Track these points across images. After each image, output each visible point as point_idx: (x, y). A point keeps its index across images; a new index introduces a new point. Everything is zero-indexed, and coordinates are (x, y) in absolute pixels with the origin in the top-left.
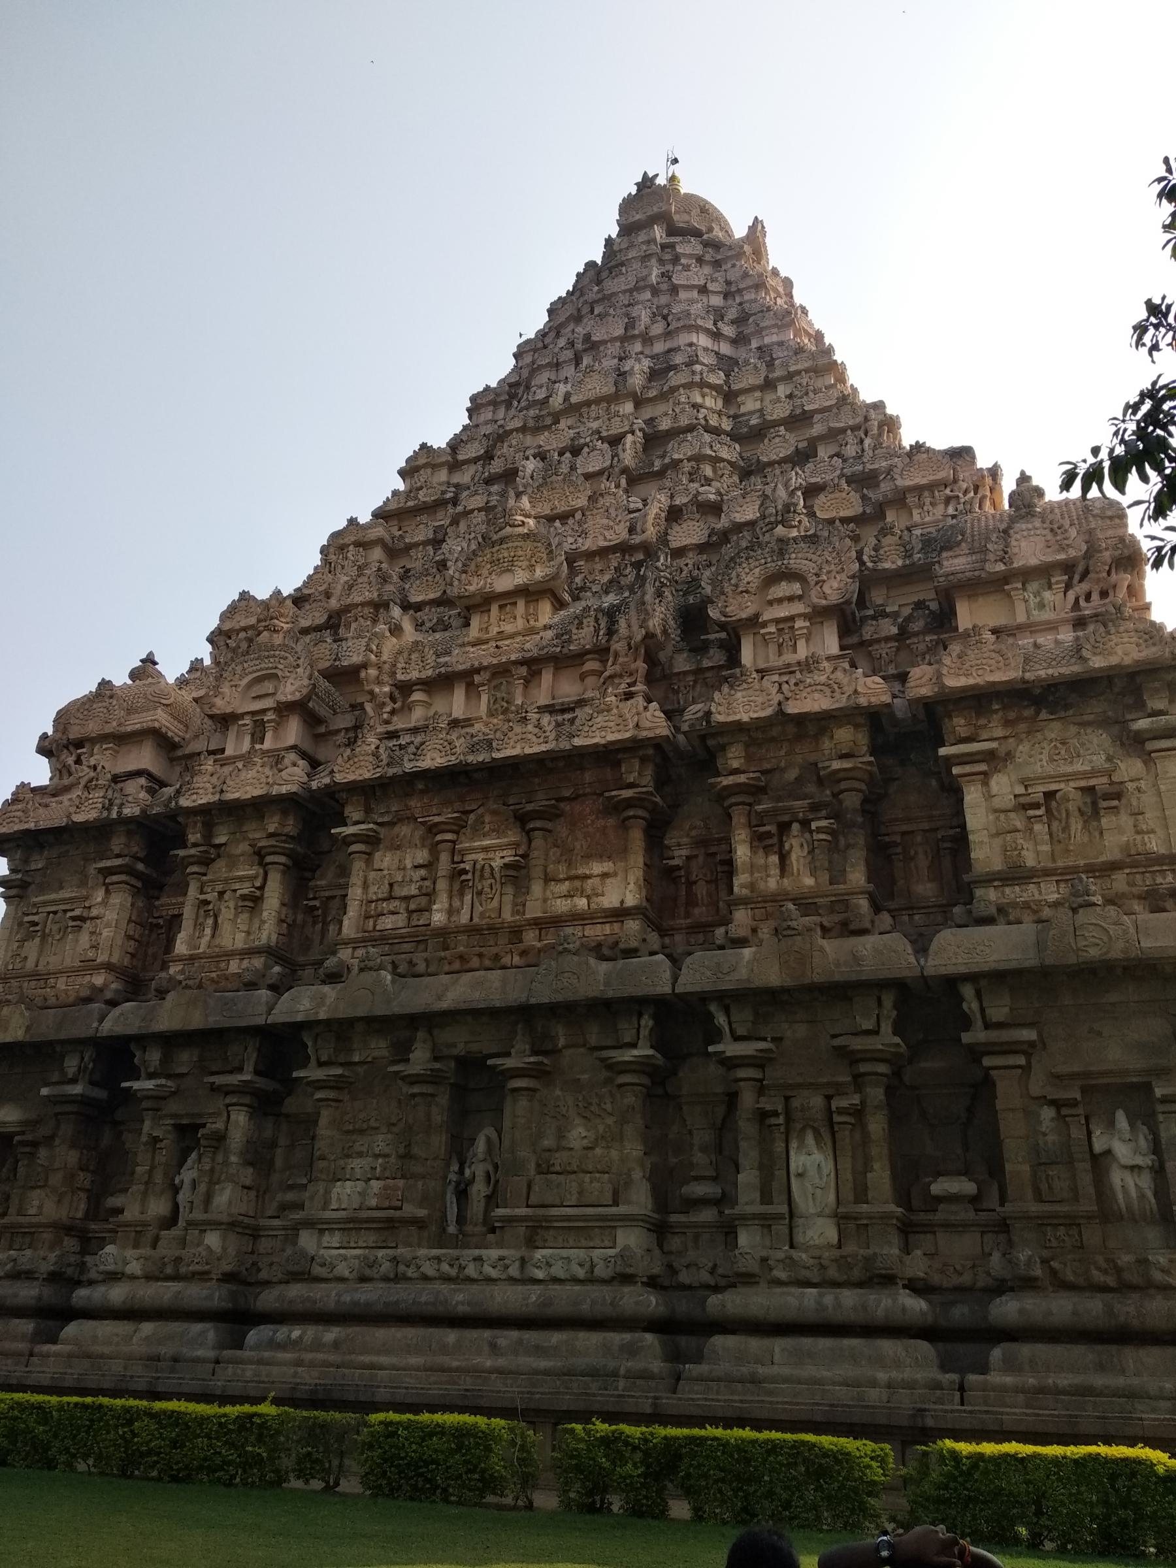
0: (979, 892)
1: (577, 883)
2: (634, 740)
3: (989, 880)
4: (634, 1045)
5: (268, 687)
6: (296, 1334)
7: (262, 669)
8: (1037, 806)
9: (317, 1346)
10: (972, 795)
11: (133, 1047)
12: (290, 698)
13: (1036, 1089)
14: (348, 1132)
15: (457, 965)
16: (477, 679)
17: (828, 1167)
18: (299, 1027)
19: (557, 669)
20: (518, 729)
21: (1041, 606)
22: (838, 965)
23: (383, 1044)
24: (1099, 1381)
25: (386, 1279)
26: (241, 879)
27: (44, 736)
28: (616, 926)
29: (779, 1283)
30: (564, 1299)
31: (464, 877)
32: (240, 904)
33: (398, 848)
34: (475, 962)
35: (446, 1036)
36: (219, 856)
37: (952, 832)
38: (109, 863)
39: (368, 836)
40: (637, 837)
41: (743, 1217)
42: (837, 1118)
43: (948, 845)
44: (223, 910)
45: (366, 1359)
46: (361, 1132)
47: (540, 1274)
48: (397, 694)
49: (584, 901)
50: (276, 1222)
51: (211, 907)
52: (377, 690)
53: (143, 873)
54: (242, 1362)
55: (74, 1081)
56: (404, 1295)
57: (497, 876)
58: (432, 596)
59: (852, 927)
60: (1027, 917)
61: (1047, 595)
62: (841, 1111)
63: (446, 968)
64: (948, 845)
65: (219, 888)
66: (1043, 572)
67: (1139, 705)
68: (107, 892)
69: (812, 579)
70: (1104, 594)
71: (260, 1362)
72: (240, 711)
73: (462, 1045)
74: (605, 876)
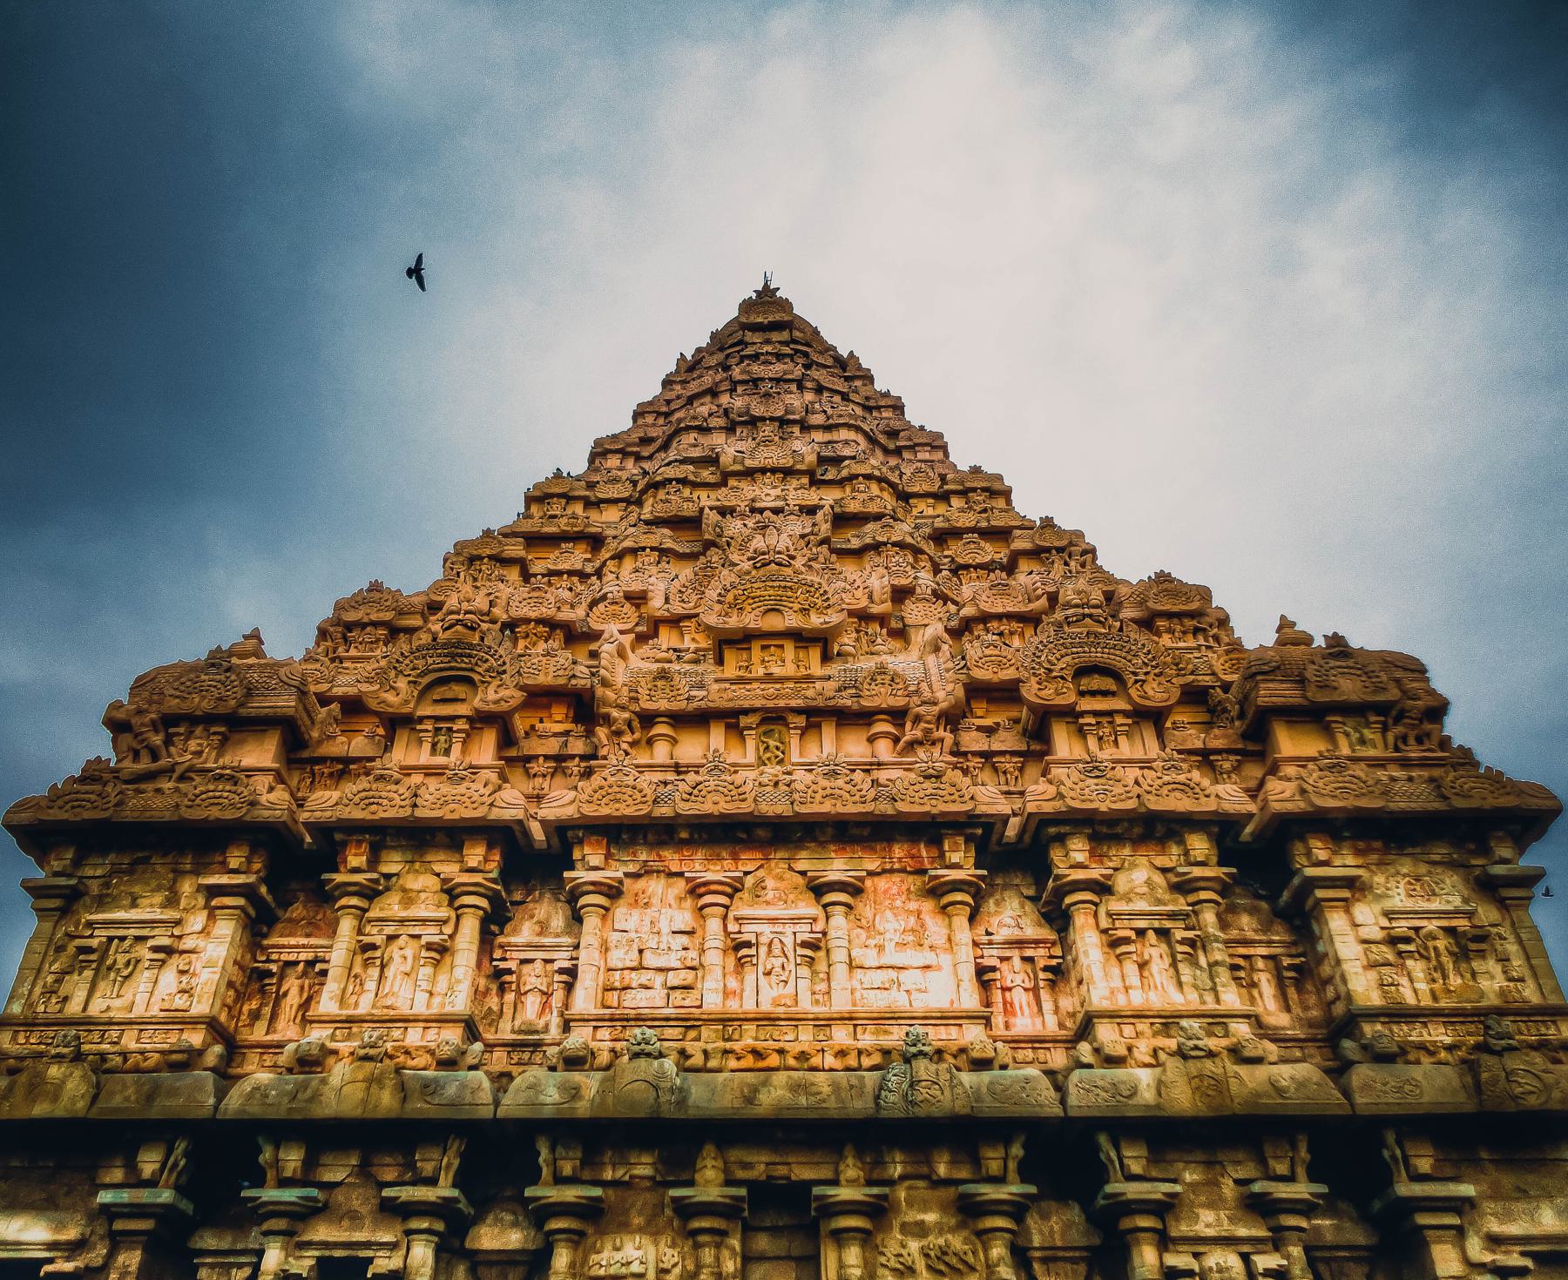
1: (893, 974)
4: (1000, 1180)
5: (458, 690)
7: (451, 669)
10: (1336, 921)
15: (749, 1061)
16: (744, 721)
19: (839, 725)
21: (1362, 741)
23: (646, 1159)
26: (424, 921)
27: (117, 706)
28: (954, 1031)
31: (744, 952)
32: (424, 953)
36: (388, 889)
38: (224, 880)
43: (1292, 974)
51: (378, 953)
52: (615, 713)
53: (262, 899)
57: (791, 955)
59: (1247, 1053)
61: (1366, 732)
63: (733, 1063)
64: (1292, 974)
65: (389, 930)
68: (211, 917)
72: (420, 713)
73: (763, 1167)
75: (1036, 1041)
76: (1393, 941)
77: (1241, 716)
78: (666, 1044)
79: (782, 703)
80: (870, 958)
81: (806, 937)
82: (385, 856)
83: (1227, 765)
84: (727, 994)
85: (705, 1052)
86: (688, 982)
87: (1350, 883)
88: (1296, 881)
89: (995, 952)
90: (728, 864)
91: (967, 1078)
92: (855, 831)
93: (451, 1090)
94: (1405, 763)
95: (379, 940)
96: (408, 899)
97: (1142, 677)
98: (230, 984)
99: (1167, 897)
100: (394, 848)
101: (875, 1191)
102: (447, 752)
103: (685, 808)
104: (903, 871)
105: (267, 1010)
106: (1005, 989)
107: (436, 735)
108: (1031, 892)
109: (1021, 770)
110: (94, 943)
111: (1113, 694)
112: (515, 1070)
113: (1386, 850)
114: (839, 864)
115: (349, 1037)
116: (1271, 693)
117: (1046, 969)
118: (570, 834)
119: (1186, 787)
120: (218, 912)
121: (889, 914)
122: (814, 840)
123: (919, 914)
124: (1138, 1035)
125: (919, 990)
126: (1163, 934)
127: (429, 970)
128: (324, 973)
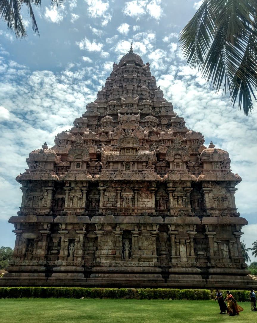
0: (207, 211)
2: (156, 180)
3: (209, 209)
6: (100, 275)
9: (104, 277)
10: (206, 196)
11: (59, 224)
12: (86, 160)
16: (123, 163)
17: (185, 250)
18: (94, 224)
20: (135, 175)
21: (217, 167)
22: (189, 221)
24: (224, 280)
25: (114, 266)
26: (78, 194)
29: (179, 267)
30: (146, 269)
33: (109, 192)
35: (122, 226)
40: (153, 196)
42: (187, 243)
45: (115, 279)
47: (141, 266)
48: (107, 163)
50: (87, 256)
54: (91, 280)
55: (46, 230)
56: (119, 269)
62: (188, 242)
63: (121, 215)
67: (230, 185)
68: (48, 193)
69: (183, 156)
70: (225, 167)
71: (95, 280)
75: (163, 211)
76: (214, 199)
79: (129, 160)
81: (132, 197)
82: (71, 184)
83: (197, 169)
84: (120, 205)
91: (152, 218)
94: (222, 171)
95: (72, 197)
102: (79, 167)
103: (114, 179)
105: (57, 205)
110: (32, 197)
112: (92, 214)
114: (137, 186)
115: (69, 211)
116: (205, 158)
119: (188, 176)
123: (147, 193)
124: (176, 211)
126: (182, 197)
128: (65, 200)
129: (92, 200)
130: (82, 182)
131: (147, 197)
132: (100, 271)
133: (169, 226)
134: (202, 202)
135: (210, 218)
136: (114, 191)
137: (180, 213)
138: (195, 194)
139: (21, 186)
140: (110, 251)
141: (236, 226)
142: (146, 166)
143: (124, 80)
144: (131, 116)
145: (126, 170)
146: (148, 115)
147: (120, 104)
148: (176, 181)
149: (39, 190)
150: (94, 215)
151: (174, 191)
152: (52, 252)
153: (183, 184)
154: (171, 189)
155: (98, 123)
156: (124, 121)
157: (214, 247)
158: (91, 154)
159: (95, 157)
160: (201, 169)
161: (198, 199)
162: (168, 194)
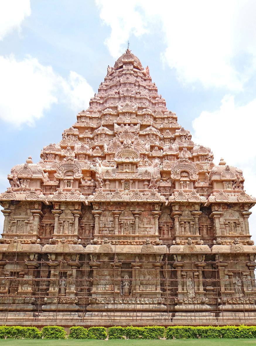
1: (145, 229)
8: (227, 224)
10: (217, 221)
11: (48, 255)
13: (226, 273)
14: (100, 275)
16: (122, 181)
21: (228, 187)
23: (107, 258)
25: (112, 304)
26: (69, 219)
31: (121, 225)
32: (70, 224)
33: (106, 216)
34: (126, 243)
36: (62, 213)
37: (210, 226)
39: (100, 213)
41: (180, 293)
42: (195, 276)
44: (66, 225)
46: (103, 275)
48: (103, 181)
49: (147, 233)
51: (62, 224)
53: (41, 214)
57: (129, 226)
58: (98, 155)
60: (225, 244)
61: (229, 185)
62: (196, 275)
64: (209, 228)
65: (64, 220)
66: (229, 181)
67: (243, 208)
70: (238, 187)
74: (151, 228)
75: (167, 239)
76: (225, 224)
77: (210, 180)
78: (110, 240)
80: (142, 226)
81: (132, 222)
82: (61, 206)
84: (119, 232)
85: (115, 241)
86: (113, 230)
87: (220, 214)
88: (212, 213)
89: (162, 224)
90: (119, 209)
91: (155, 247)
92: (140, 204)
93: (77, 248)
94: (235, 192)
95: (62, 222)
96: (66, 215)
97: (192, 174)
98: (38, 228)
99: (191, 216)
100: (63, 205)
101: (141, 263)
104: (148, 210)
105: (44, 232)
106: (163, 230)
107: (68, 183)
108: (169, 213)
109: (170, 190)
110: (15, 221)
111: (187, 177)
112: (86, 243)
113: (228, 208)
114: (137, 209)
115: (59, 238)
116: (214, 178)
117: (170, 227)
118: (92, 203)
120: (35, 216)
121: (145, 218)
122: (134, 205)
123: (150, 218)
125: (149, 232)
126: (189, 223)
127: (71, 227)
128: (54, 226)
129: (85, 227)
130: (73, 204)
131: (149, 223)
132: (96, 309)
133: (175, 256)
134: (212, 228)
135: (221, 246)
136: (111, 215)
137: (187, 241)
138: (204, 219)
139: (3, 208)
140: (108, 286)
141: (249, 256)
142: (148, 185)
143: (120, 85)
144: (129, 127)
145: (125, 190)
146: (149, 126)
147: (116, 114)
148: (183, 203)
149: (24, 213)
150: (88, 244)
151: (180, 215)
152: (41, 287)
153: (191, 206)
154: (177, 212)
155: (91, 136)
156: (121, 132)
157: (224, 280)
158: (84, 172)
159: (88, 175)
160: (210, 190)
161: (207, 225)
162: (173, 220)
